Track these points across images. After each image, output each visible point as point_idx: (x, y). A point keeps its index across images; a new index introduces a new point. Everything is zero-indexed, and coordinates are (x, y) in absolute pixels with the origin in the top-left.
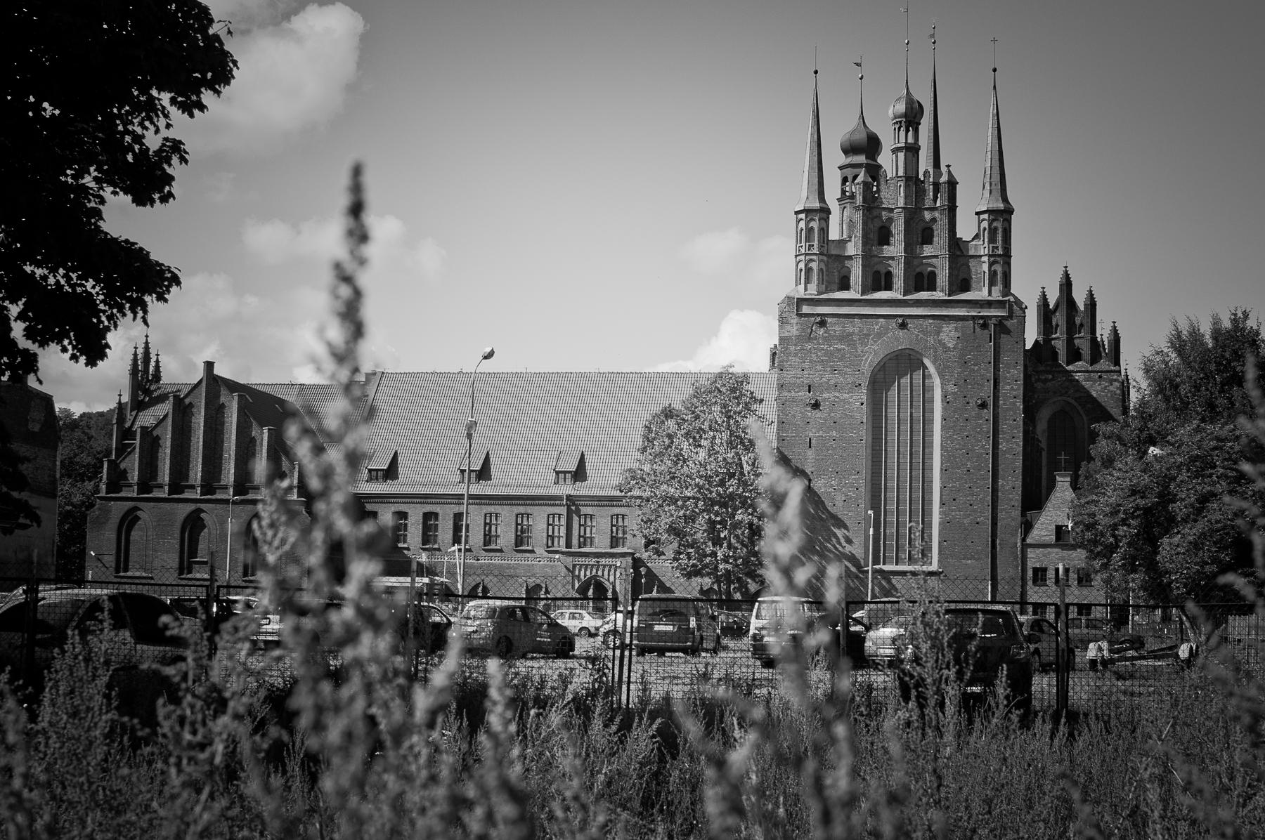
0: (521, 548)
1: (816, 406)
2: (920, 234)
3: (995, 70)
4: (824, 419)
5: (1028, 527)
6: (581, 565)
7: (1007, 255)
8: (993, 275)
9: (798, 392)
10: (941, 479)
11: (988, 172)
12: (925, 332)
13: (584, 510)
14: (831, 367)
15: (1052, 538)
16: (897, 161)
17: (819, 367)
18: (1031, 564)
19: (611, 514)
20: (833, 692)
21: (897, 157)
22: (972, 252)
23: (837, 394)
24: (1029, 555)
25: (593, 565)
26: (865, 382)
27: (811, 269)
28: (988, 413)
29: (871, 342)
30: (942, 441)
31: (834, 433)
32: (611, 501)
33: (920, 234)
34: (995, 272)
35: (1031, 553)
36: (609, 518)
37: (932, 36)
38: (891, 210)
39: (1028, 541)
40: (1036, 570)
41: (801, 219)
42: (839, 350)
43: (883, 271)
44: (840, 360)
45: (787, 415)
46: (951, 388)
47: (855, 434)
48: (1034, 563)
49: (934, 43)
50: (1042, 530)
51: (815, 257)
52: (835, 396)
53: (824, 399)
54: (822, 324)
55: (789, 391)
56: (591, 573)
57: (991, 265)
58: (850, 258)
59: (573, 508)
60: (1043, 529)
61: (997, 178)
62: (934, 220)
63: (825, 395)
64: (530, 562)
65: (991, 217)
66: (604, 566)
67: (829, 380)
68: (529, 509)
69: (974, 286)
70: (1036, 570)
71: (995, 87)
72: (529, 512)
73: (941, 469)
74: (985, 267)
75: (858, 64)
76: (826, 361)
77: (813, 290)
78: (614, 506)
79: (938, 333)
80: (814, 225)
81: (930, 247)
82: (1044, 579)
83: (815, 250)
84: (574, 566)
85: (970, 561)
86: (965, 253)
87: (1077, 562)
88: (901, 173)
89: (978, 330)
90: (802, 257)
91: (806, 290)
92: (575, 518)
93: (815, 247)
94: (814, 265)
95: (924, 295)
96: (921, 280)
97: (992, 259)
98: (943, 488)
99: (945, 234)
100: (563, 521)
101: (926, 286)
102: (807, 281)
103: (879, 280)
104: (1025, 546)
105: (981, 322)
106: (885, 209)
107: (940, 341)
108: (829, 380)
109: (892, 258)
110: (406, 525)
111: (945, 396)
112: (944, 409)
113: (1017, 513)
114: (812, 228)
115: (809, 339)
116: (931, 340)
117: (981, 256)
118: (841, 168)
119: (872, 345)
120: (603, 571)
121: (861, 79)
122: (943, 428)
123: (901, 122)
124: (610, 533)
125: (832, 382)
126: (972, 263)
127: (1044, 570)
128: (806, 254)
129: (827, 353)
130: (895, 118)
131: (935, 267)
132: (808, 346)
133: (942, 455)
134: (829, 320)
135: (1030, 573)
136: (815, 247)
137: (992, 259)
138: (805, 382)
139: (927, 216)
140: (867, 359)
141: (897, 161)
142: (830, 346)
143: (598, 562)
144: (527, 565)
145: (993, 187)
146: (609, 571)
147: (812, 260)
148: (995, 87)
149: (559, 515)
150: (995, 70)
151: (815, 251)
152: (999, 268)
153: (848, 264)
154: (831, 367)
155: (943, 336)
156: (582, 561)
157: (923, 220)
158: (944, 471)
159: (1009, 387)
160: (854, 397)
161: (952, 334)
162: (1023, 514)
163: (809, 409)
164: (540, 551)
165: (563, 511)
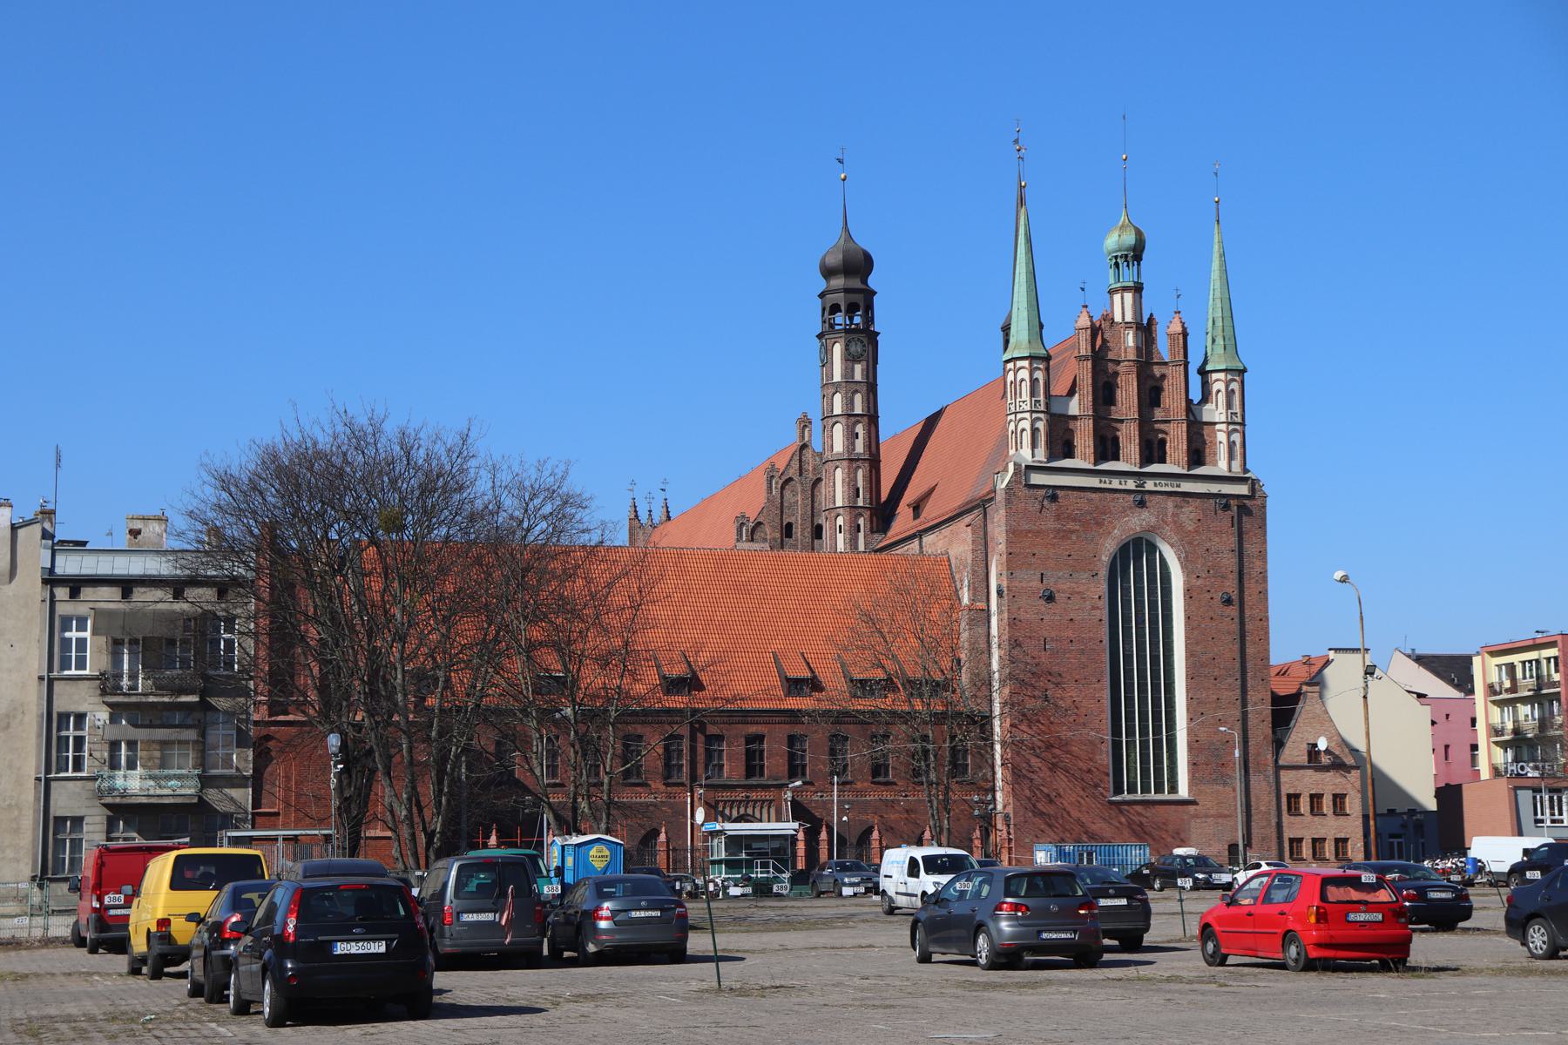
0: (629, 781)
2: (1151, 394)
5: (1279, 744)
6: (726, 802)
7: (1243, 424)
8: (1231, 445)
11: (1219, 323)
13: (712, 730)
15: (1303, 760)
16: (1123, 303)
18: (1285, 790)
20: (1314, 944)
21: (1122, 298)
22: (1205, 419)
24: (1283, 779)
25: (741, 801)
27: (1038, 429)
28: (1233, 611)
32: (746, 716)
33: (1151, 394)
34: (1234, 442)
35: (1285, 776)
37: (1016, 141)
38: (1118, 362)
39: (1281, 762)
40: (1289, 796)
43: (1110, 436)
48: (1290, 788)
49: (1019, 150)
51: (1042, 416)
54: (1054, 498)
56: (738, 813)
57: (1229, 434)
58: (1075, 418)
59: (697, 726)
60: (1294, 751)
61: (1229, 332)
62: (1163, 376)
64: (642, 800)
65: (1229, 377)
66: (756, 801)
68: (640, 729)
69: (1208, 459)
71: (1218, 221)
73: (1187, 675)
74: (1222, 437)
75: (841, 161)
77: (1041, 454)
78: (748, 723)
80: (1039, 375)
81: (1159, 410)
82: (1320, 807)
83: (1042, 408)
84: (717, 802)
86: (1198, 419)
88: (1129, 318)
91: (1033, 457)
92: (700, 738)
93: (1042, 403)
94: (1041, 425)
95: (1155, 468)
96: (1153, 450)
100: (685, 745)
101: (1110, 457)
102: (1034, 445)
103: (1107, 447)
104: (1278, 768)
105: (1224, 501)
106: (1111, 360)
109: (1122, 421)
110: (762, 752)
113: (1267, 728)
114: (1037, 379)
117: (1215, 423)
118: (822, 295)
120: (754, 808)
121: (844, 180)
123: (1126, 256)
126: (1206, 430)
128: (1032, 412)
130: (1120, 250)
131: (1166, 434)
134: (1060, 493)
135: (1284, 800)
136: (1042, 403)
139: (1157, 371)
141: (1123, 303)
143: (747, 797)
144: (641, 803)
145: (1226, 340)
146: (762, 808)
147: (1039, 419)
151: (1042, 409)
153: (1072, 425)
156: (726, 795)
157: (1153, 376)
162: (1274, 732)
164: (657, 785)
165: (685, 731)
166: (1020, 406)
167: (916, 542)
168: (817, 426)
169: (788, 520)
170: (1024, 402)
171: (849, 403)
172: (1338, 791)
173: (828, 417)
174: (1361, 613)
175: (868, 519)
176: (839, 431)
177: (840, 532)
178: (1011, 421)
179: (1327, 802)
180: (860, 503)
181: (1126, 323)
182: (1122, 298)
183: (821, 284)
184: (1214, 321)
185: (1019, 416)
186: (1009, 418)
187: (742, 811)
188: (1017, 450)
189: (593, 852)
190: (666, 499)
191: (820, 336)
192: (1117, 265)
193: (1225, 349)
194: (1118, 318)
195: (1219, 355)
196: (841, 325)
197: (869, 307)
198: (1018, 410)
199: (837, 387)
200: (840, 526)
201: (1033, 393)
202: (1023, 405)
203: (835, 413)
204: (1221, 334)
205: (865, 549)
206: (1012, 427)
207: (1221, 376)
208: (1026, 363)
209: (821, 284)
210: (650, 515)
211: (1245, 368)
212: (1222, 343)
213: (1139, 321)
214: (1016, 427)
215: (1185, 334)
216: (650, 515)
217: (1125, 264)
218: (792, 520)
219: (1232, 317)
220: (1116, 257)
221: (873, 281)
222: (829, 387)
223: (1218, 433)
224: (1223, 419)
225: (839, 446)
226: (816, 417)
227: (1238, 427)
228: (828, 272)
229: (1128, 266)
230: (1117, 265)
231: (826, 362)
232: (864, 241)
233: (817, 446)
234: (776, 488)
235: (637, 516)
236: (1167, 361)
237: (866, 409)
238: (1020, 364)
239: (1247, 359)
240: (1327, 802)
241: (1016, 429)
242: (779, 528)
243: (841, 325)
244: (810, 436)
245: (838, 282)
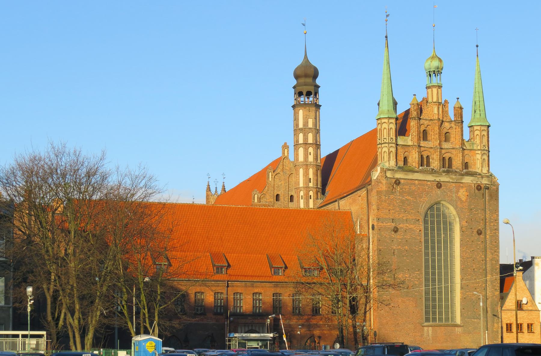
1: (396, 230)
3: (477, 46)
4: (402, 239)
9: (386, 223)
10: (461, 274)
12: (451, 191)
14: (404, 209)
15: (514, 307)
17: (398, 209)
19: (252, 292)
23: (407, 225)
26: (422, 219)
29: (424, 196)
30: (461, 253)
31: (407, 247)
36: (252, 295)
39: (503, 309)
41: (379, 124)
42: (407, 200)
44: (408, 205)
45: (382, 236)
46: (465, 224)
47: (417, 248)
48: (507, 320)
50: (510, 302)
52: (406, 226)
53: (401, 228)
55: (382, 223)
57: (482, 155)
63: (401, 225)
67: (403, 217)
70: (507, 325)
71: (477, 56)
72: (203, 291)
73: (461, 269)
74: (479, 156)
75: (304, 25)
76: (401, 205)
79: (457, 192)
85: (476, 320)
87: (527, 320)
89: (476, 191)
90: (387, 145)
97: (483, 152)
98: (462, 279)
99: (458, 138)
107: (459, 197)
108: (403, 217)
111: (461, 228)
112: (462, 235)
115: (392, 193)
116: (454, 195)
117: (476, 150)
118: (294, 87)
119: (424, 198)
122: (461, 245)
124: (252, 304)
125: (405, 218)
127: (511, 325)
129: (402, 202)
132: (392, 196)
133: (461, 261)
134: (402, 181)
137: (483, 152)
138: (391, 217)
140: (422, 206)
141: (432, 93)
142: (403, 197)
145: (481, 111)
148: (477, 56)
149: (241, 293)
150: (477, 46)
151: (394, 142)
152: (485, 157)
154: (404, 209)
155: (460, 194)
158: (462, 270)
159: (492, 224)
160: (416, 227)
161: (465, 193)
163: (393, 233)
166: (383, 140)
167: (336, 203)
168: (292, 149)
169: (278, 193)
170: (385, 139)
171: (306, 138)
172: (530, 322)
173: (297, 145)
174: (514, 238)
175: (315, 193)
176: (301, 151)
177: (302, 199)
178: (379, 148)
179: (525, 327)
180: (311, 185)
181: (434, 102)
182: (432, 91)
183: (294, 82)
184: (475, 102)
185: (383, 145)
186: (379, 146)
187: (250, 328)
188: (382, 161)
189: (148, 344)
190: (224, 183)
191: (294, 107)
192: (430, 75)
193: (480, 116)
194: (430, 100)
195: (478, 118)
196: (303, 101)
197: (316, 93)
198: (382, 142)
199: (301, 130)
200: (302, 196)
201: (389, 134)
202: (385, 140)
203: (300, 143)
204: (478, 108)
205: (314, 207)
206: (380, 150)
207: (478, 128)
208: (386, 121)
209: (294, 82)
210: (216, 190)
211: (489, 124)
212: (479, 112)
213: (440, 101)
214: (382, 150)
215: (461, 108)
216: (216, 190)
217: (434, 75)
218: (279, 193)
219: (484, 101)
220: (430, 72)
221: (318, 81)
222: (297, 130)
223: (477, 155)
224: (479, 148)
225: (301, 158)
226: (291, 144)
227: (485, 152)
228: (297, 77)
229: (435, 76)
230: (430, 75)
231: (296, 119)
232: (314, 62)
233: (292, 158)
234: (272, 178)
235: (210, 190)
236: (453, 120)
237: (314, 141)
238: (383, 121)
239: (490, 121)
240: (525, 327)
241: (382, 151)
242: (273, 196)
243: (303, 101)
244: (288, 154)
245: (302, 80)
